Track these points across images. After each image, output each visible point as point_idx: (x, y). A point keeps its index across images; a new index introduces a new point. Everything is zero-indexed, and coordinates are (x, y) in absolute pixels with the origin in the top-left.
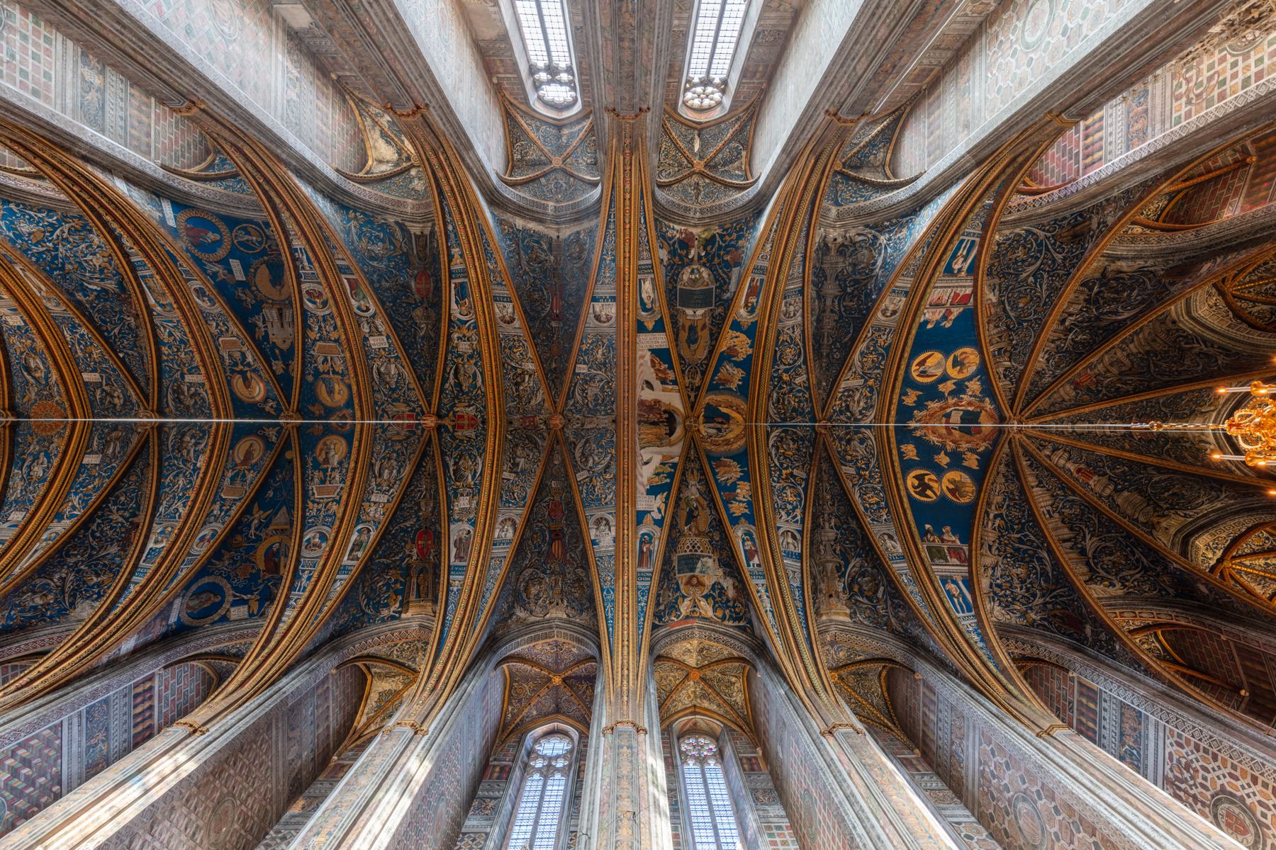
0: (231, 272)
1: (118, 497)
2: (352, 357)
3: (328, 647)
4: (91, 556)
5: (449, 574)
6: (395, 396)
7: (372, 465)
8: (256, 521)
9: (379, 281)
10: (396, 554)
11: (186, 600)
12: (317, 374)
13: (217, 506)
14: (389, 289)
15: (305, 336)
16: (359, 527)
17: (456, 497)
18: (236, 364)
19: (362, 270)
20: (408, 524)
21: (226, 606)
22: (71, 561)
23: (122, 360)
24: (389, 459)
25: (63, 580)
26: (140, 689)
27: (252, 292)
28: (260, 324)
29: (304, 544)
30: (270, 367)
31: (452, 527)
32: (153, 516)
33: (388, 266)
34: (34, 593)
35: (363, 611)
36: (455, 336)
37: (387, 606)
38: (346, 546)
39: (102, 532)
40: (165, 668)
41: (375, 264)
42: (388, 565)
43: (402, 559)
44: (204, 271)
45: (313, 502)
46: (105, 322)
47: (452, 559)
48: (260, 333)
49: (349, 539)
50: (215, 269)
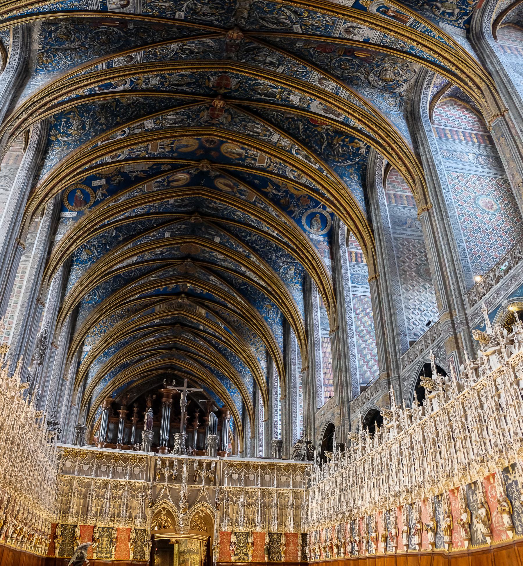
0: (101, 186)
1: (242, 236)
2: (161, 139)
3: (369, 190)
4: (274, 250)
5: (348, 126)
6: (194, 116)
7: (248, 135)
8: (274, 191)
9: (101, 125)
10: (323, 137)
11: (312, 231)
12: (172, 151)
13: (259, 205)
14: (106, 118)
15: (144, 158)
16: (294, 152)
17: (289, 101)
18: (163, 185)
19: (94, 137)
20: (301, 127)
21: (324, 212)
22: (274, 258)
23: (158, 225)
24: (246, 126)
25: (283, 262)
26: (354, 259)
27: (113, 176)
28: (135, 174)
29: (296, 179)
30: (165, 171)
31: (312, 110)
32: (257, 229)
33: (88, 118)
34: (287, 273)
35: (355, 164)
36: (144, 86)
37: (358, 149)
38: (305, 163)
39: (261, 244)
40: (348, 246)
41: (87, 126)
42: (328, 143)
43: (328, 134)
44: (102, 201)
45: (268, 167)
46: (135, 230)
47: (338, 119)
48: (142, 175)
49: (300, 160)
50: (99, 194)
